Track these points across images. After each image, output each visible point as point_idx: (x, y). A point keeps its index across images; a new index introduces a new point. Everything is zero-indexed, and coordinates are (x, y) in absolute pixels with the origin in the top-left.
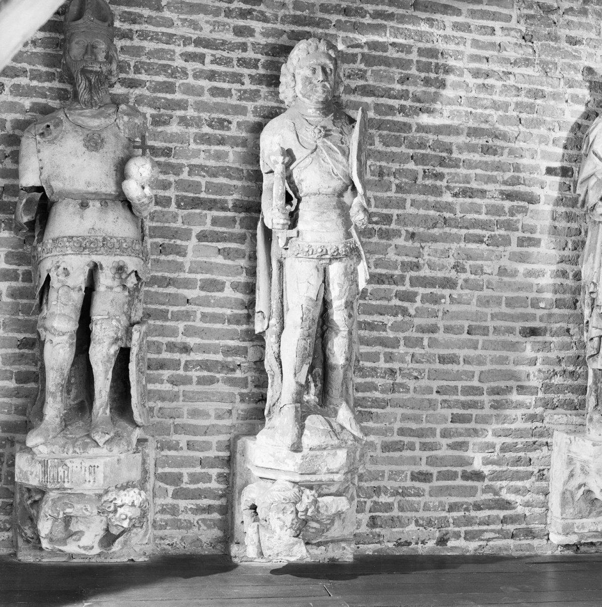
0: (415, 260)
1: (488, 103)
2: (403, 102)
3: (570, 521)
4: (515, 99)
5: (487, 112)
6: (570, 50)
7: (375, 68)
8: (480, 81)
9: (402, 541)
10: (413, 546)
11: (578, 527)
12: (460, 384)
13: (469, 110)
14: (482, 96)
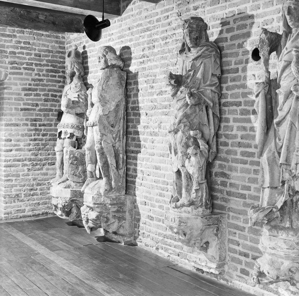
0: (147, 125)
1: (167, 51)
2: (143, 59)
3: (186, 253)
4: (176, 46)
5: (167, 55)
6: (194, 13)
7: (136, 48)
8: (164, 42)
9: (146, 244)
10: (149, 247)
11: (189, 257)
12: (161, 179)
13: (162, 55)
14: (165, 48)
